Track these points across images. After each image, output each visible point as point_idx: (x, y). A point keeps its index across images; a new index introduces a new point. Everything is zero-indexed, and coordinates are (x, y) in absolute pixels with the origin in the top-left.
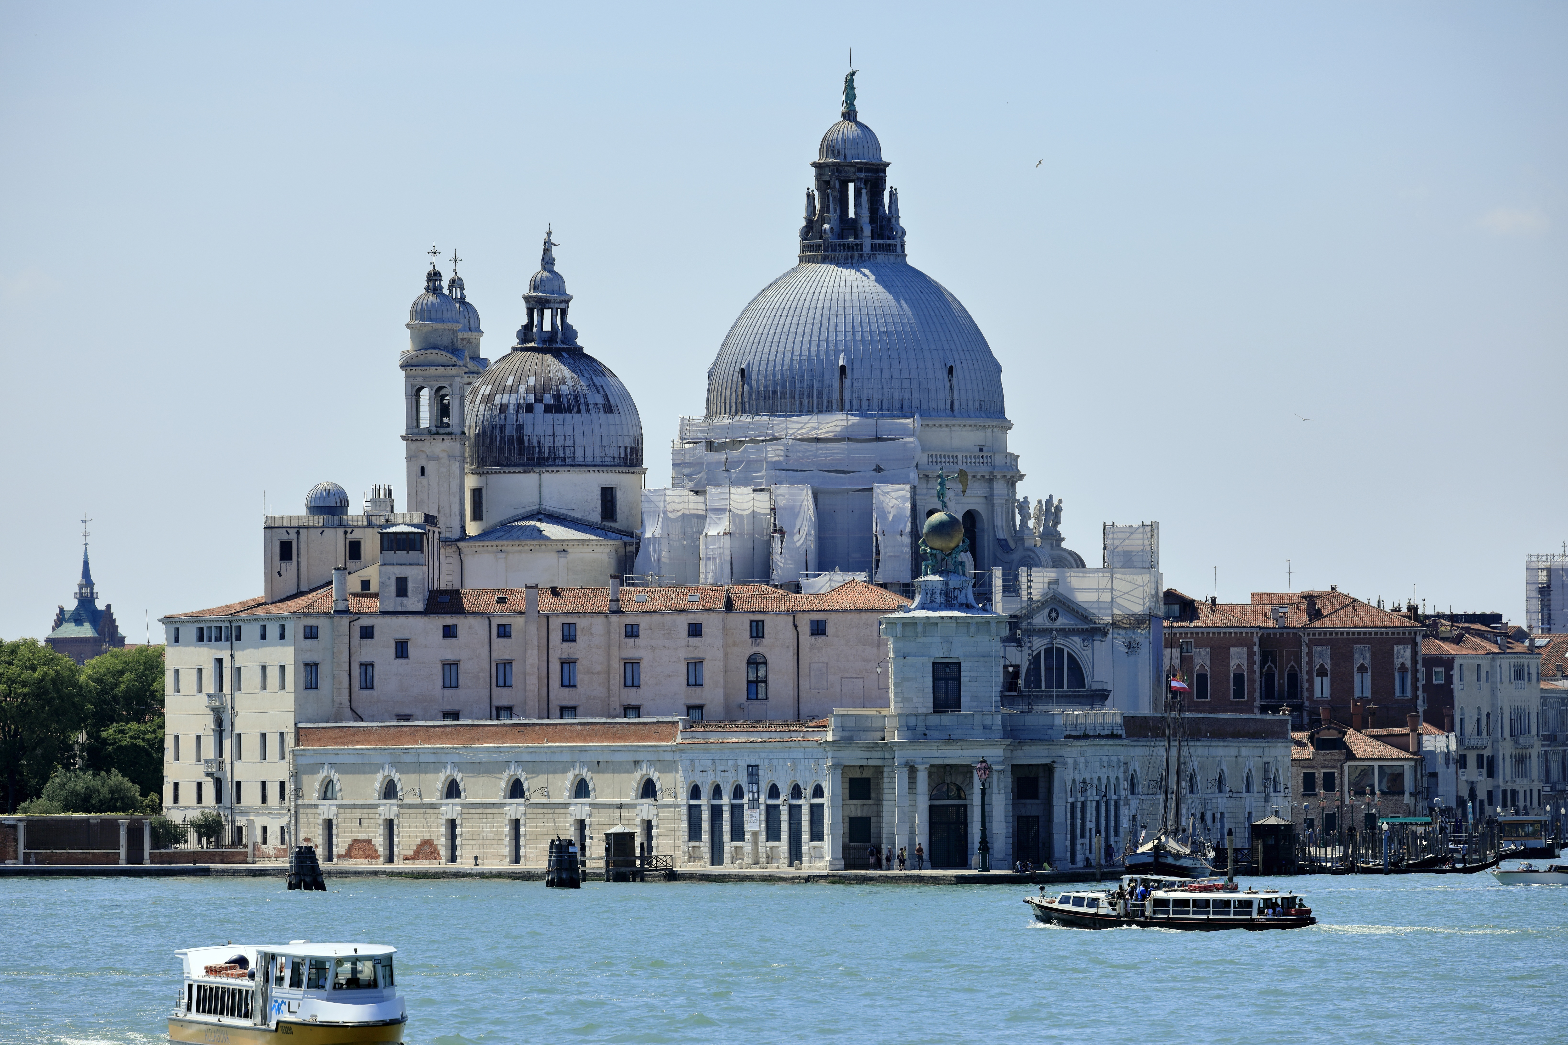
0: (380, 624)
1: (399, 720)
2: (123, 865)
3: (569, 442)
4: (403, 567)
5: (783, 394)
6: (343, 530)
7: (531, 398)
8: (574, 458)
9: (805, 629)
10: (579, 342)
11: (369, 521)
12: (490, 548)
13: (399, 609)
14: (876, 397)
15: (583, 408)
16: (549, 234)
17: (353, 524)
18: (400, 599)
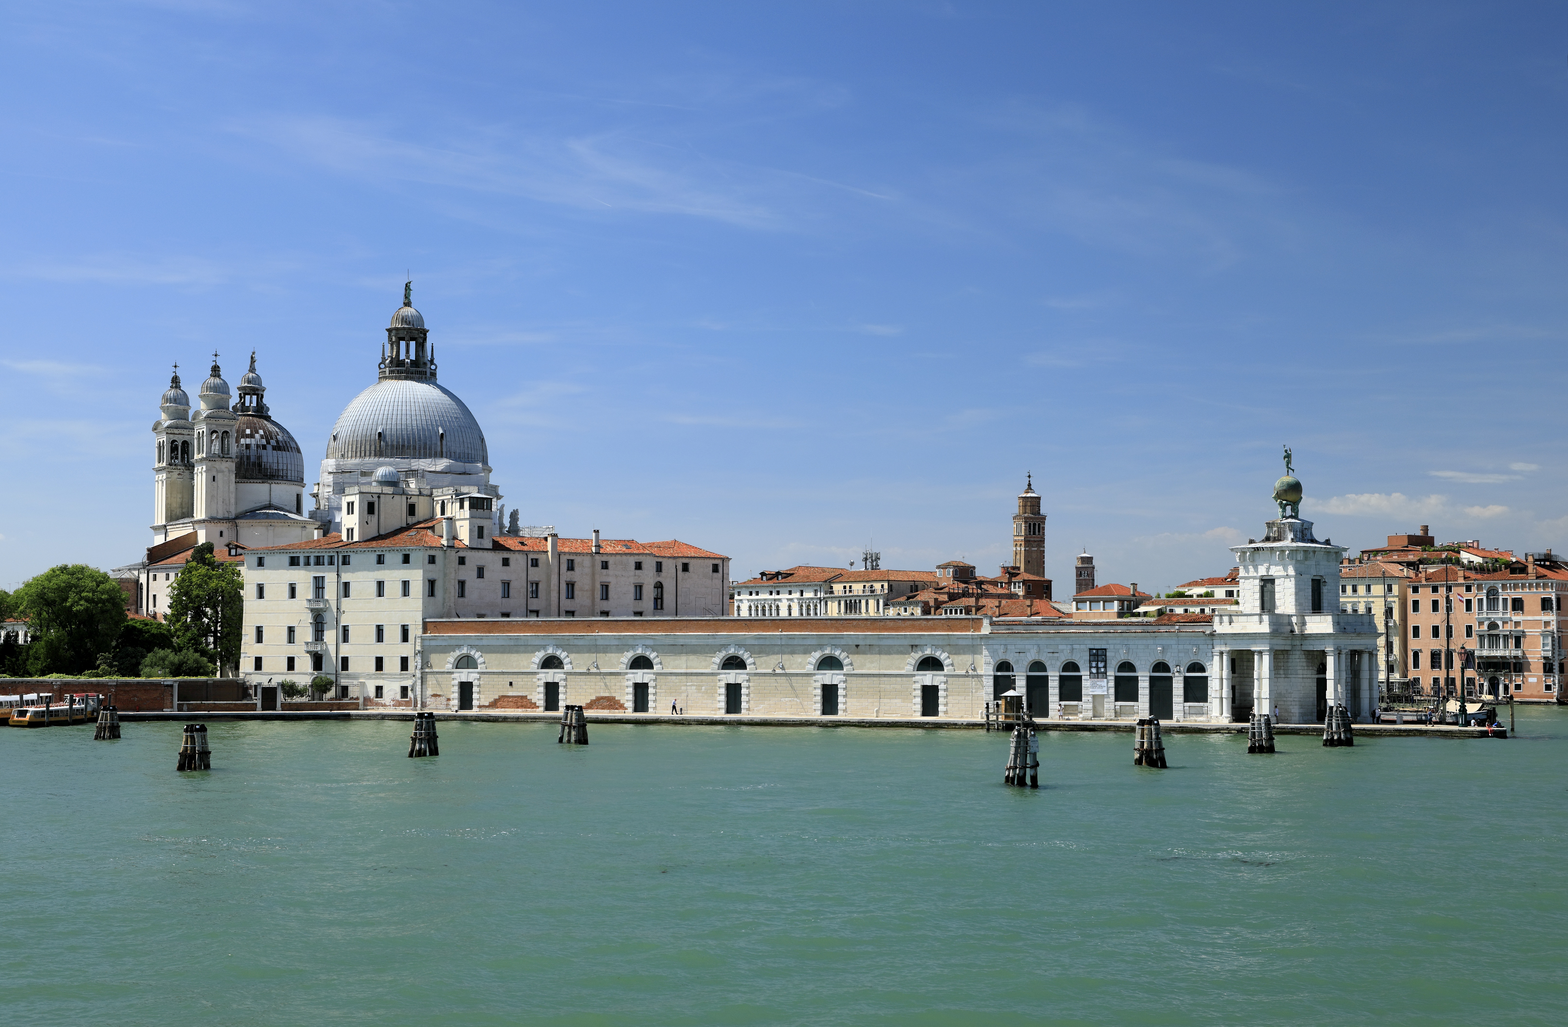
0: (469, 555)
1: (478, 617)
2: (259, 712)
3: (285, 468)
4: (482, 520)
5: (409, 447)
6: (405, 496)
7: (264, 442)
8: (287, 476)
9: (680, 568)
10: (270, 413)
11: (420, 492)
12: (263, 524)
13: (479, 547)
14: (458, 451)
15: (289, 449)
16: (254, 353)
17: (410, 493)
18: (480, 540)
